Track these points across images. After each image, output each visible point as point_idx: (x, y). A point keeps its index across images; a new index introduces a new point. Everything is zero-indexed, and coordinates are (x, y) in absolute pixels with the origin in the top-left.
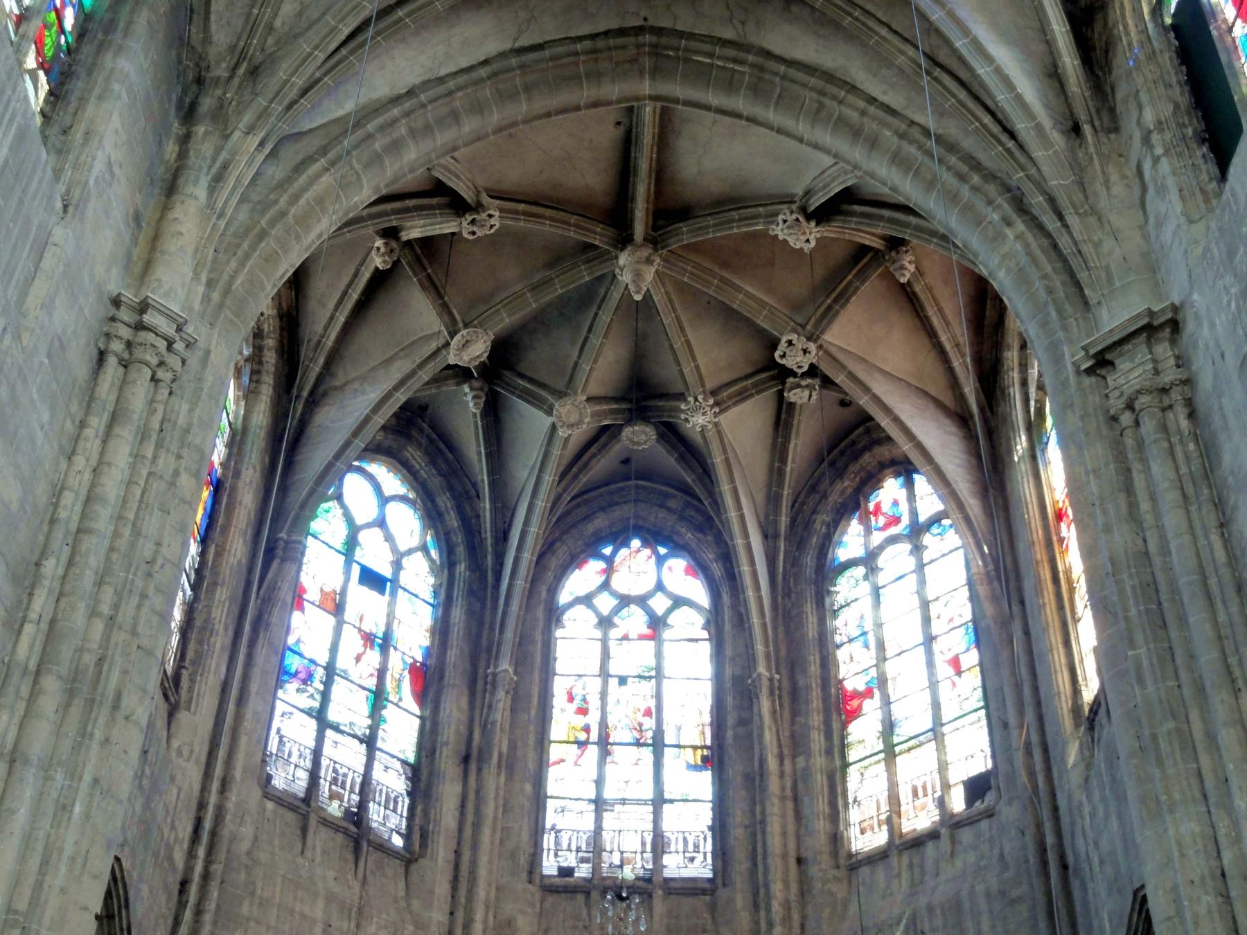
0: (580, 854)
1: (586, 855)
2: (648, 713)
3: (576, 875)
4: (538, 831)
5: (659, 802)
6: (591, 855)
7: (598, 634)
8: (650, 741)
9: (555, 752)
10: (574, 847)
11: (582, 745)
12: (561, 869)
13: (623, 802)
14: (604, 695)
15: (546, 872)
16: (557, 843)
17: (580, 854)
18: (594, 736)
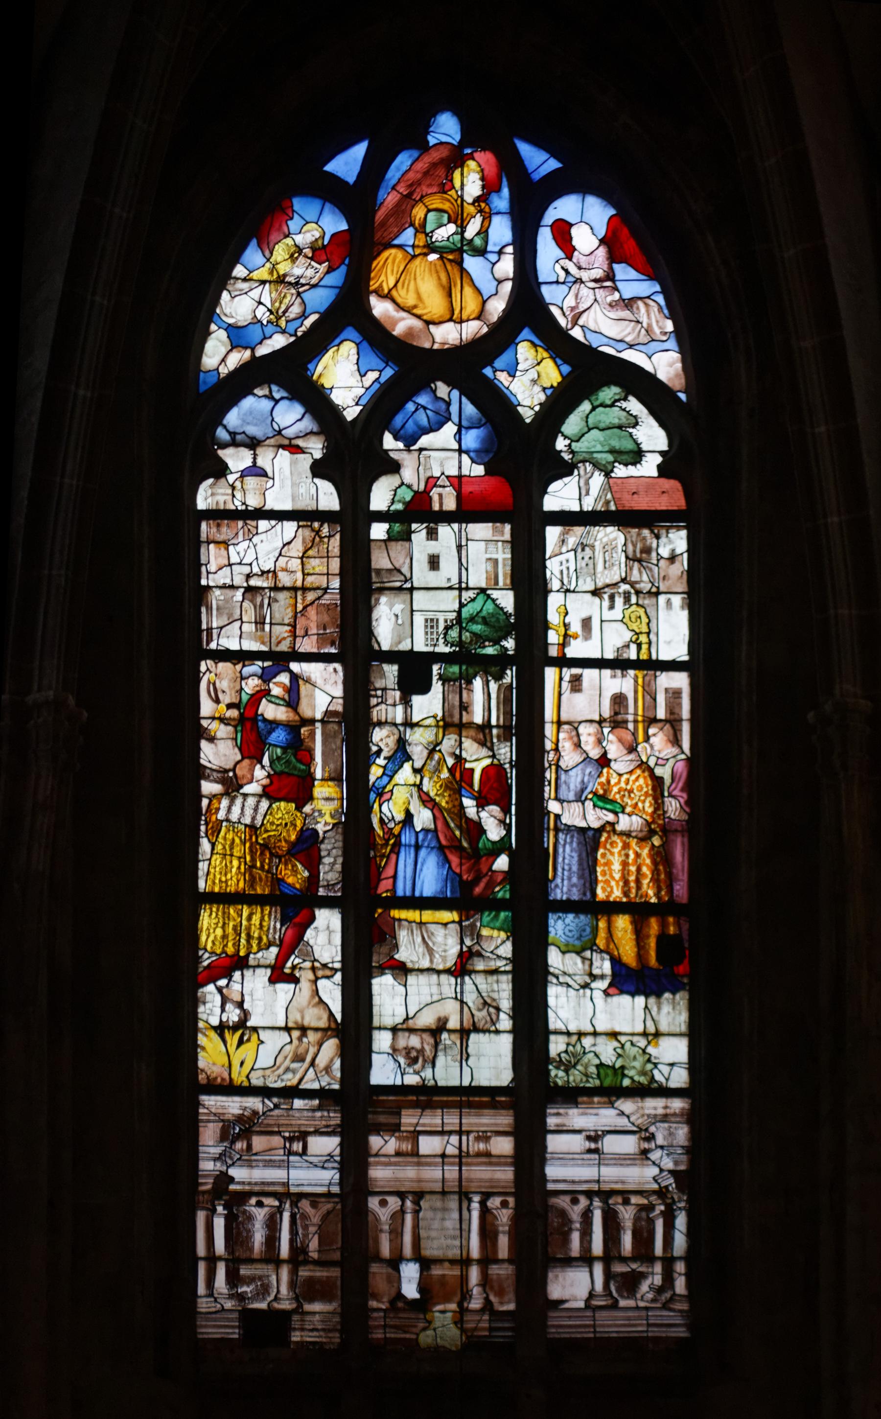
0: (304, 1273)
1: (320, 1273)
2: (493, 790)
3: (296, 1337)
4: (178, 1190)
5: (536, 1091)
6: (335, 1273)
7: (328, 497)
8: (502, 893)
9: (212, 929)
10: (285, 1250)
11: (297, 909)
12: (248, 1317)
13: (428, 1096)
14: (354, 719)
15: (209, 1331)
16: (236, 1233)
17: (304, 1273)
18: (330, 869)
